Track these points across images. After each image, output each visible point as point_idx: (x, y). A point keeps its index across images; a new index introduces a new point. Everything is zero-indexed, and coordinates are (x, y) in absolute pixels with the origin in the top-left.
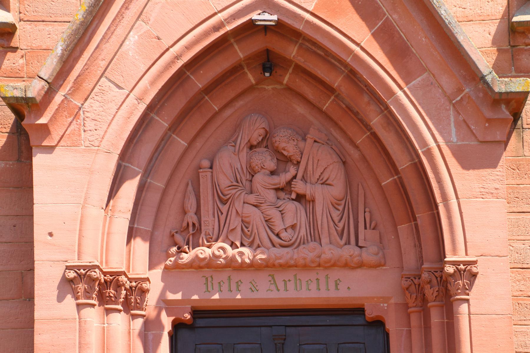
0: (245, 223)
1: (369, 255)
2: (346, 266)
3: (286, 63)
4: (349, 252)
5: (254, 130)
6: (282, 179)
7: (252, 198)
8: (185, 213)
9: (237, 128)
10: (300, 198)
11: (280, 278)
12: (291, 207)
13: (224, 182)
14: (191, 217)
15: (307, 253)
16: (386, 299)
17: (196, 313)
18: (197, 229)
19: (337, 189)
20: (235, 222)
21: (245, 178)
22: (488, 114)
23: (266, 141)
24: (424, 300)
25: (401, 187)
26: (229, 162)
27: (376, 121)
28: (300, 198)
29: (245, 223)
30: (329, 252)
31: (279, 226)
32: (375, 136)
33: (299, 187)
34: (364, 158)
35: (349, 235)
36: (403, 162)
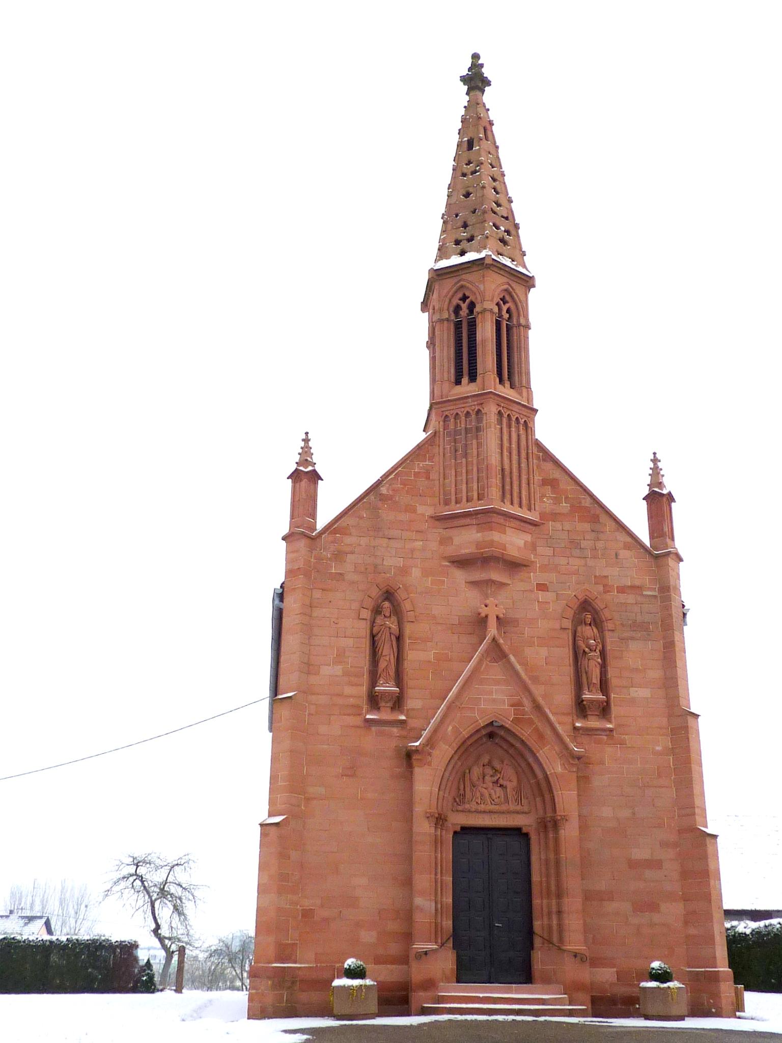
0: (482, 795)
1: (526, 809)
2: (518, 813)
3: (497, 734)
4: (519, 808)
5: (485, 759)
6: (495, 778)
7: (485, 786)
8: (459, 789)
9: (478, 758)
10: (501, 786)
11: (493, 816)
12: (498, 790)
13: (475, 778)
14: (462, 792)
15: (504, 807)
16: (530, 826)
17: (463, 828)
18: (464, 795)
19: (515, 783)
20: (478, 795)
21: (481, 777)
22: (572, 762)
23: (490, 763)
24: (546, 827)
25: (538, 784)
26: (476, 771)
27: (531, 760)
28: (501, 786)
29: (482, 795)
30: (512, 807)
31: (494, 797)
32: (529, 764)
33: (501, 782)
34: (523, 771)
35: (519, 801)
36: (540, 775)
